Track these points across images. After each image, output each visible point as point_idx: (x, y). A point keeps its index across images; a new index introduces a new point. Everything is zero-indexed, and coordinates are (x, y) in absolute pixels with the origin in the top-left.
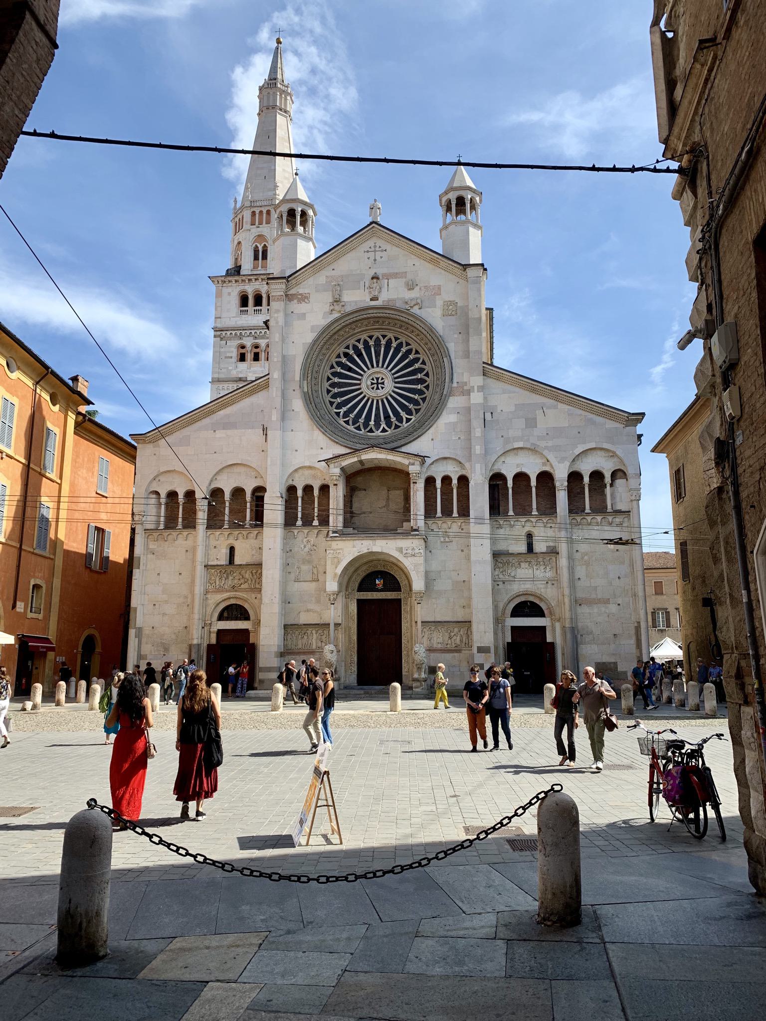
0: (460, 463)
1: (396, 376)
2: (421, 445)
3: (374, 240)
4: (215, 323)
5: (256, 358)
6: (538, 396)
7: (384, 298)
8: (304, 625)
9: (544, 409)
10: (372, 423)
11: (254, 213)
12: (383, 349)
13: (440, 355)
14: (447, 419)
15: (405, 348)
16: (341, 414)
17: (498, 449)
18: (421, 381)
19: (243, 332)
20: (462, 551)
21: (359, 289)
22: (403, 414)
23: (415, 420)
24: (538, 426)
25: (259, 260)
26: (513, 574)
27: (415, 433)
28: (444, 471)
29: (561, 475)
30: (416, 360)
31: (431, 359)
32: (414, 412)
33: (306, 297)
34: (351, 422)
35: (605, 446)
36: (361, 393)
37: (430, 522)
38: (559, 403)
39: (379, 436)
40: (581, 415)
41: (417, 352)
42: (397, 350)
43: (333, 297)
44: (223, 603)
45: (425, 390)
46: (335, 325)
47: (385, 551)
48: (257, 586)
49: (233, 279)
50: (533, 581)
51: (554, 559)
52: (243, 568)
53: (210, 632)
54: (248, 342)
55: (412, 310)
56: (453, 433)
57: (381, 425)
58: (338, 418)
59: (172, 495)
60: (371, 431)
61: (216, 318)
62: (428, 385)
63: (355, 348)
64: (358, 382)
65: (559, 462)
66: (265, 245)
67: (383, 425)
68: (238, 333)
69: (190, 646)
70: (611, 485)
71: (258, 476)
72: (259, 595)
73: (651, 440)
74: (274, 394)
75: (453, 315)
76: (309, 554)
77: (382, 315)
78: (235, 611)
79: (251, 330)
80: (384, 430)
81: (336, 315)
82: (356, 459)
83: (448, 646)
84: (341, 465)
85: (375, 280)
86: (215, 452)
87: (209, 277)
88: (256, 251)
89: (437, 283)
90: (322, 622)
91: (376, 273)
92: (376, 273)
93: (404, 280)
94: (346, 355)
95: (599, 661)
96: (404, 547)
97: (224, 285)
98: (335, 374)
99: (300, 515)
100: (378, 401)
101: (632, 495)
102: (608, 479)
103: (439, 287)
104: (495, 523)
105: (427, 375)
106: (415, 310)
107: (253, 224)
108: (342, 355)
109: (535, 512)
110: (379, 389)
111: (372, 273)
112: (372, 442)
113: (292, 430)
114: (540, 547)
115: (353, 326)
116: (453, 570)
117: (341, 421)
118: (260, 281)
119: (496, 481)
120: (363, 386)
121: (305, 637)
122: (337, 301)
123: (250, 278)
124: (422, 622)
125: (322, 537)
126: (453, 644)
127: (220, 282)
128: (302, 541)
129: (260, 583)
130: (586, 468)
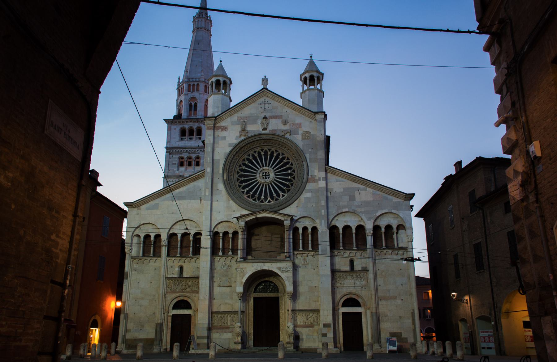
0: (313, 220)
2: (291, 210)
4: (167, 145)
5: (190, 164)
6: (356, 184)
7: (270, 128)
8: (223, 312)
9: (360, 190)
10: (263, 197)
11: (189, 85)
12: (269, 157)
13: (301, 160)
14: (306, 195)
15: (282, 156)
17: (334, 212)
18: (290, 174)
19: (183, 150)
20: (314, 269)
21: (256, 124)
22: (280, 192)
23: (287, 196)
24: (356, 200)
25: (192, 111)
26: (343, 283)
27: (287, 203)
28: (304, 225)
29: (369, 226)
30: (288, 163)
31: (296, 163)
32: (286, 191)
34: (250, 197)
35: (393, 211)
36: (257, 180)
38: (367, 188)
39: (267, 204)
40: (380, 194)
41: (288, 159)
43: (241, 128)
44: (176, 299)
45: (293, 179)
46: (242, 143)
47: (271, 269)
48: (196, 289)
49: (178, 121)
50: (354, 286)
51: (366, 274)
52: (187, 279)
53: (168, 316)
54: (185, 156)
55: (285, 136)
56: (309, 203)
57: (268, 198)
59: (147, 237)
60: (262, 202)
61: (167, 142)
62: (294, 177)
63: (253, 156)
64: (255, 174)
65: (368, 220)
66: (196, 103)
67: (269, 199)
68: (180, 151)
69: (157, 324)
70: (397, 233)
71: (198, 225)
72: (197, 295)
73: (416, 210)
74: (208, 181)
75: (308, 139)
76: (226, 270)
77: (268, 138)
78: (183, 304)
79: (187, 149)
80: (269, 201)
81: (243, 138)
82: (254, 217)
83: (306, 323)
84: (245, 220)
85: (265, 119)
86: (173, 213)
87: (164, 120)
88: (190, 105)
89: (299, 122)
90: (233, 310)
91: (265, 116)
92: (265, 116)
93: (281, 120)
94: (248, 159)
95: (392, 332)
97: (172, 124)
98: (242, 170)
101: (408, 239)
102: (395, 230)
103: (301, 124)
105: (294, 171)
106: (287, 136)
107: (189, 91)
108: (246, 160)
110: (267, 178)
111: (263, 115)
112: (263, 208)
113: (217, 201)
114: (358, 266)
115: (252, 144)
116: (309, 281)
117: (245, 196)
118: (193, 122)
119: (333, 229)
120: (258, 176)
121: (224, 319)
122: (244, 130)
123: (188, 120)
124: (292, 310)
125: (234, 261)
126: (309, 323)
127: (170, 123)
128: (222, 263)
129: (198, 287)
130: (383, 223)
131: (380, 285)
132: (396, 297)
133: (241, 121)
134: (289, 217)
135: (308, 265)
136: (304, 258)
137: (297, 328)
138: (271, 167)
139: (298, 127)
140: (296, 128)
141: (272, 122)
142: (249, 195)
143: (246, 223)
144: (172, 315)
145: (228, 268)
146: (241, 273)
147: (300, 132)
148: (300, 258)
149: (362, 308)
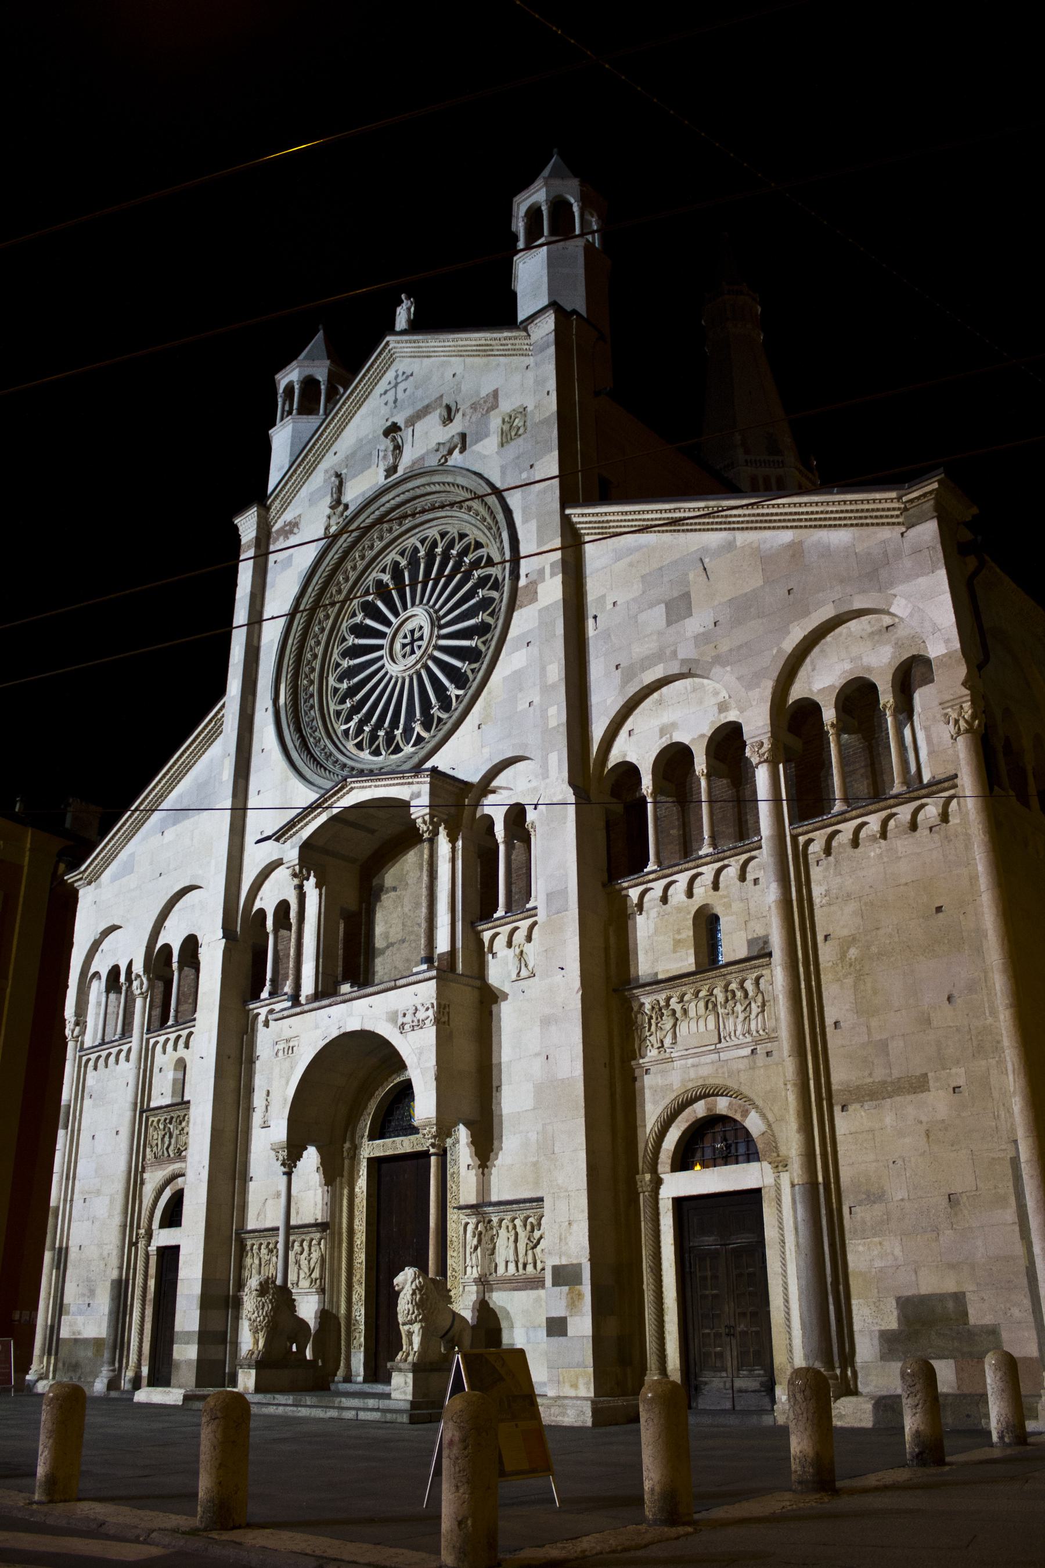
9: (706, 560)
17: (609, 702)
26: (668, 1042)
42: (446, 557)
47: (368, 1027)
53: (147, 1256)
60: (398, 750)
102: (886, 698)
103: (495, 394)
109: (706, 850)
117: (350, 745)
121: (274, 1258)
131: (836, 1024)
132: (926, 1074)
136: (518, 951)
137: (491, 1291)
142: (362, 740)
144: (155, 1248)
149: (765, 1164)
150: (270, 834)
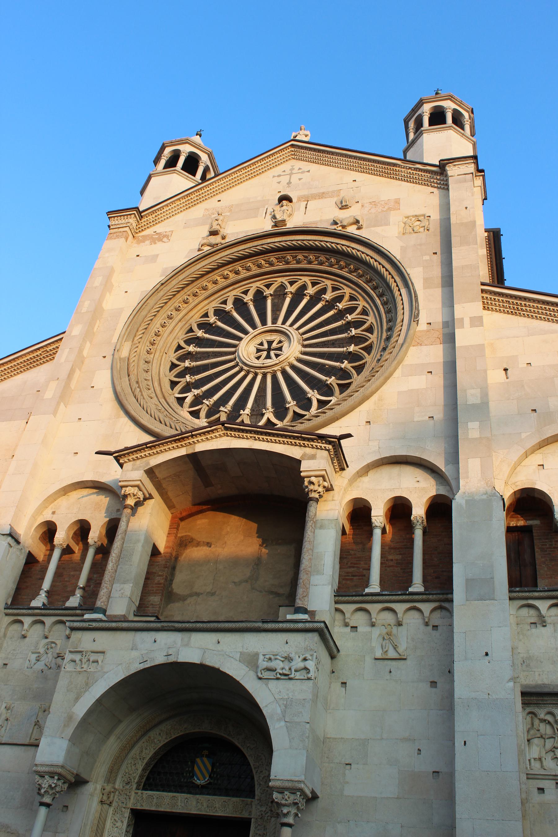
1: (305, 336)
3: (293, 162)
16: (188, 401)
17: (524, 435)
20: (433, 684)
33: (165, 236)
37: (349, 608)
47: (212, 661)
57: (263, 415)
58: (180, 408)
82: (182, 452)
85: (284, 202)
96: (262, 651)
99: (46, 585)
100: (265, 375)
104: (525, 612)
117: (184, 413)
122: (214, 233)
133: (213, 216)
134: (323, 445)
135: (402, 662)
136: (384, 631)
138: (292, 325)
139: (389, 208)
140: (383, 211)
141: (306, 208)
143: (150, 472)
145: (53, 665)
146: (80, 672)
147: (396, 218)
148: (368, 629)
150: (113, 450)
